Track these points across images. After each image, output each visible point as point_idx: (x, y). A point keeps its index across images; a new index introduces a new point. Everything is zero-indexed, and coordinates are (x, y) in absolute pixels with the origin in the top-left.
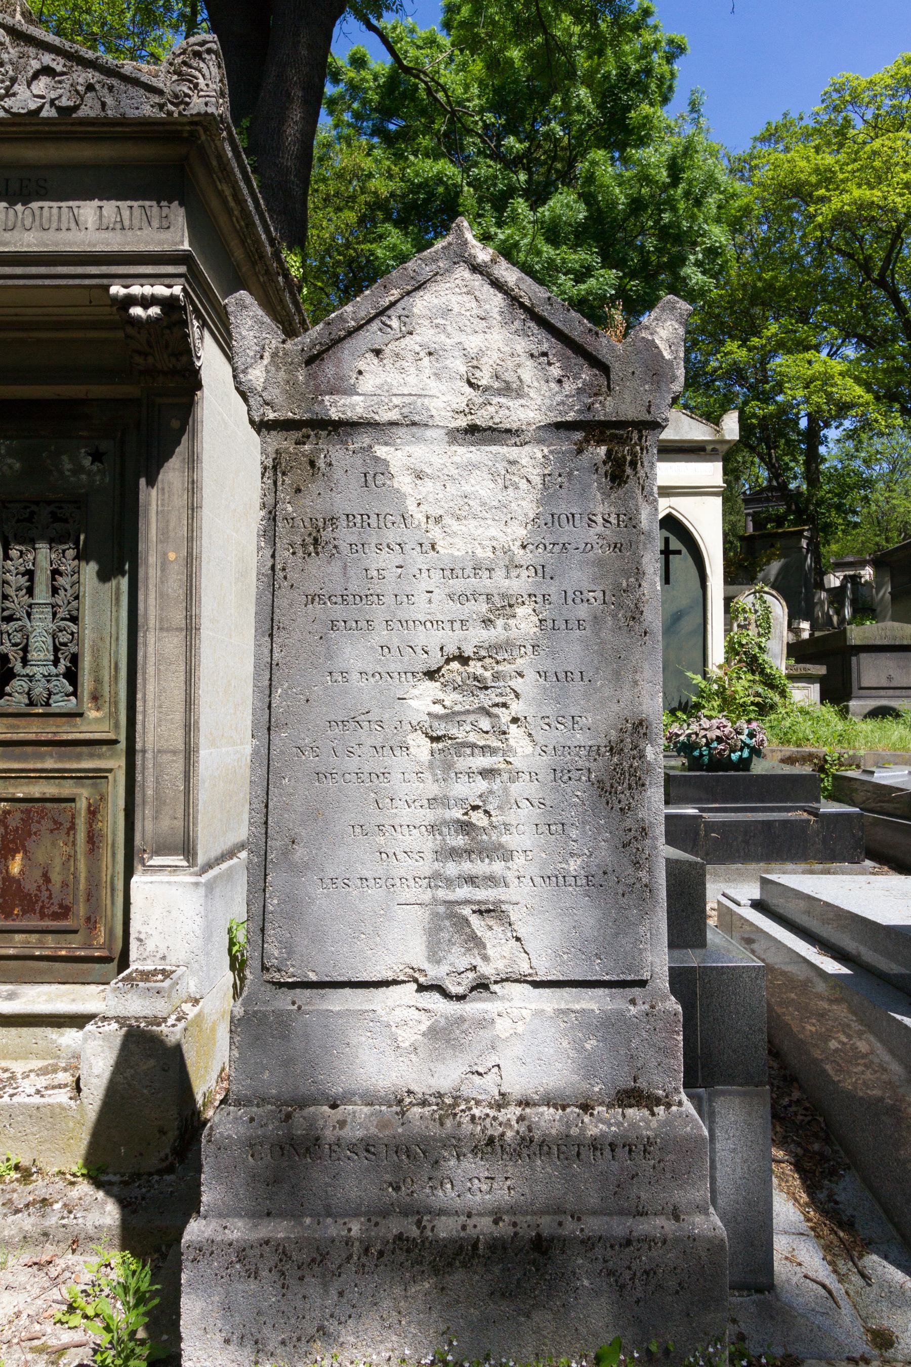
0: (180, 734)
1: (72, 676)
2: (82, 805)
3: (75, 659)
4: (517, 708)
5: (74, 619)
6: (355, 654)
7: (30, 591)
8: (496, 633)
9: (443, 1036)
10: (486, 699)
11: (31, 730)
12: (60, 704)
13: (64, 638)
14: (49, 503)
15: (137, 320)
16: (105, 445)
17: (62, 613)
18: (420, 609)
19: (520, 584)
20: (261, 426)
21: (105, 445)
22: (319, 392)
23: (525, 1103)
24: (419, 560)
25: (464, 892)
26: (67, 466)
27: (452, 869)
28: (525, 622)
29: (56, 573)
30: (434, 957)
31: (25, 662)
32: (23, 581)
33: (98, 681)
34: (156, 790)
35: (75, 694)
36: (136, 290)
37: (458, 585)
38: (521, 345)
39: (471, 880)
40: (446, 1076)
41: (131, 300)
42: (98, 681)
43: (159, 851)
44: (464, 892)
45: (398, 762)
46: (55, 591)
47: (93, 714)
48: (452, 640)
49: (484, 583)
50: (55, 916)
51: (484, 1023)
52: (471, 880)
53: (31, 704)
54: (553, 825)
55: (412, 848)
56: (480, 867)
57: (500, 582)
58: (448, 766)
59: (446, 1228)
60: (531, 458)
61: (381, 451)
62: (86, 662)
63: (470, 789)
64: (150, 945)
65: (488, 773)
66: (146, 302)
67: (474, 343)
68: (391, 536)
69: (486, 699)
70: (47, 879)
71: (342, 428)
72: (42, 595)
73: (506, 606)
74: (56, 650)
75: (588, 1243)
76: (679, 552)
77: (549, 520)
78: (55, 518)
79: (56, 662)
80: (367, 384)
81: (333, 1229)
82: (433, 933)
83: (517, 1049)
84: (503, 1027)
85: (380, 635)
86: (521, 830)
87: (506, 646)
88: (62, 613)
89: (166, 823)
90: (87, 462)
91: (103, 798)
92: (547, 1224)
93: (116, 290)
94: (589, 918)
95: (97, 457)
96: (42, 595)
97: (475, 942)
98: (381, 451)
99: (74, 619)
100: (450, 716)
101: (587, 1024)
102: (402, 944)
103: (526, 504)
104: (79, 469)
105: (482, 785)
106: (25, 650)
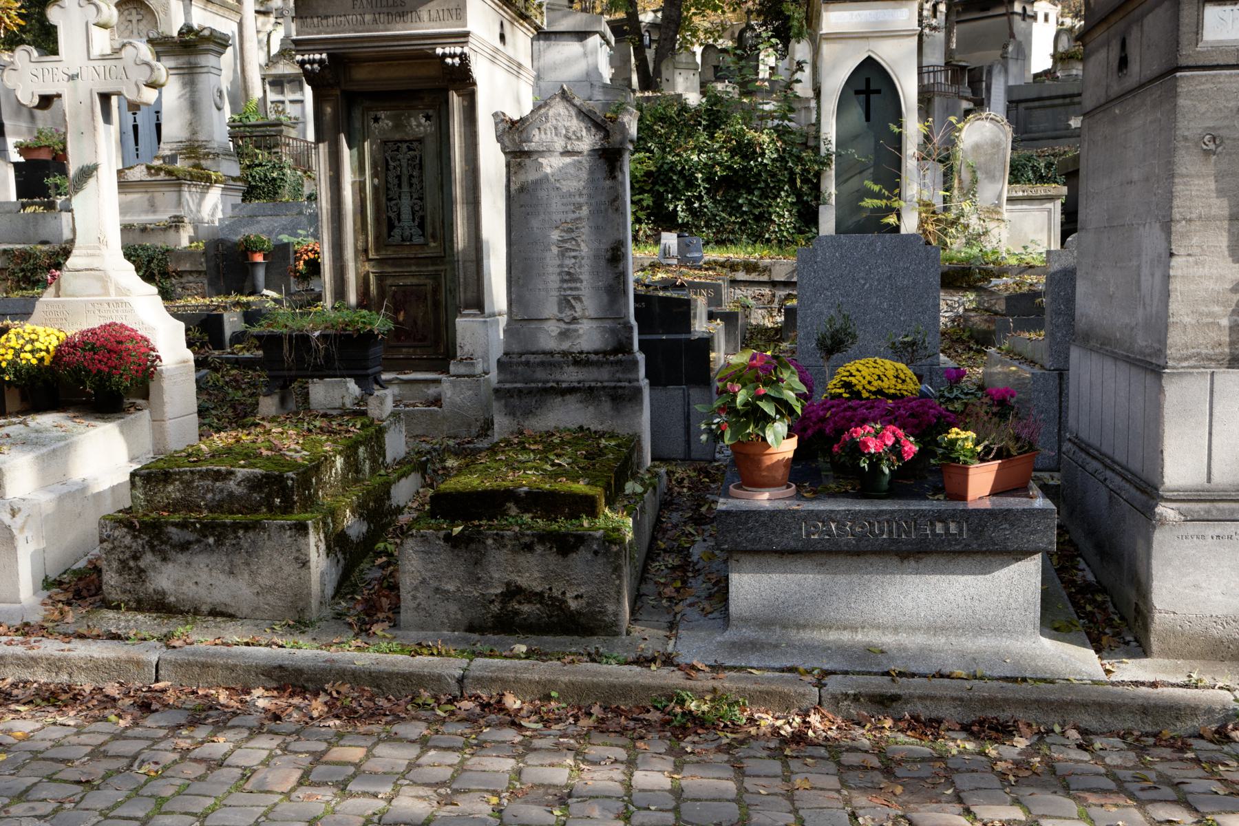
0: (473, 253)
1: (422, 226)
2: (429, 288)
3: (422, 218)
4: (584, 237)
5: (421, 199)
6: (535, 223)
7: (400, 186)
8: (577, 215)
9: (564, 335)
10: (573, 235)
11: (404, 254)
12: (416, 240)
13: (417, 208)
14: (406, 141)
15: (447, 64)
16: (430, 112)
17: (415, 196)
18: (554, 208)
19: (582, 200)
20: (505, 153)
21: (430, 112)
22: (522, 142)
23: (588, 353)
24: (553, 193)
25: (569, 292)
26: (414, 123)
27: (565, 286)
28: (585, 211)
29: (411, 176)
30: (560, 311)
31: (399, 221)
32: (396, 181)
33: (434, 228)
34: (465, 279)
35: (423, 235)
36: (447, 50)
37: (565, 201)
38: (582, 125)
39: (571, 289)
40: (565, 346)
41: (444, 56)
42: (434, 228)
43: (466, 308)
44: (569, 292)
45: (548, 254)
46: (411, 185)
47: (433, 244)
48: (563, 217)
49: (573, 200)
50: (420, 340)
51: (576, 331)
52: (571, 289)
53: (403, 240)
54: (595, 273)
55: (553, 281)
56: (573, 285)
57: (578, 199)
58: (563, 255)
59: (564, 385)
60: (585, 161)
61: (540, 160)
62: (428, 220)
63: (570, 262)
64: (466, 349)
65: (575, 257)
66: (453, 56)
67: (567, 124)
68: (545, 186)
69: (573, 235)
70: (415, 323)
71: (528, 154)
72: (405, 189)
73: (580, 207)
74: (413, 214)
75: (604, 388)
76: (878, 92)
77: (592, 180)
78: (410, 149)
79: (414, 220)
80: (536, 139)
81: (533, 385)
82: (560, 304)
83: (585, 337)
84: (581, 332)
85: (542, 216)
86: (585, 275)
87: (579, 219)
88: (415, 196)
89: (469, 295)
90: (423, 120)
91: (439, 285)
92: (593, 384)
93: (439, 51)
94: (605, 298)
95: (428, 118)
96: (405, 189)
97: (573, 307)
98: (540, 160)
99: (421, 199)
100: (564, 241)
101: (605, 330)
102: (550, 308)
103: (584, 175)
104: (419, 125)
105: (573, 261)
106: (399, 215)
